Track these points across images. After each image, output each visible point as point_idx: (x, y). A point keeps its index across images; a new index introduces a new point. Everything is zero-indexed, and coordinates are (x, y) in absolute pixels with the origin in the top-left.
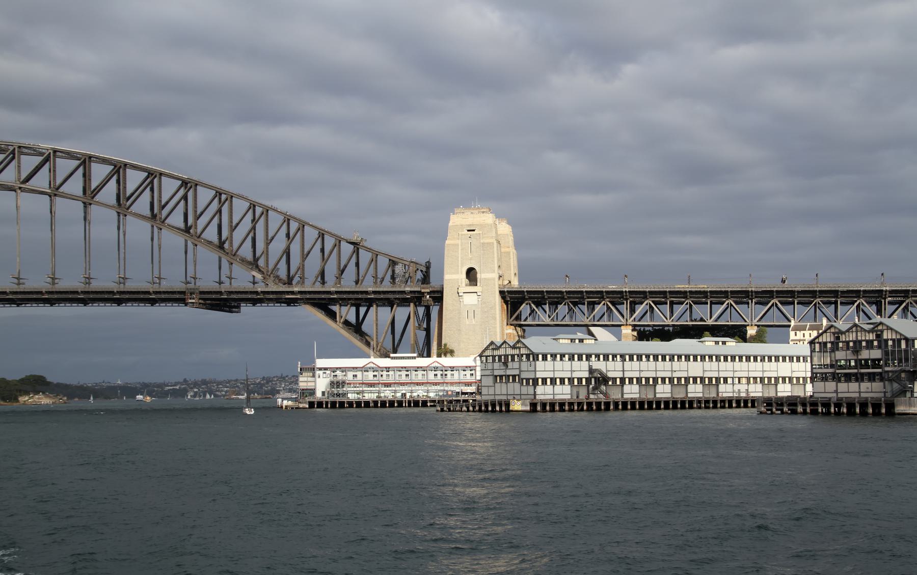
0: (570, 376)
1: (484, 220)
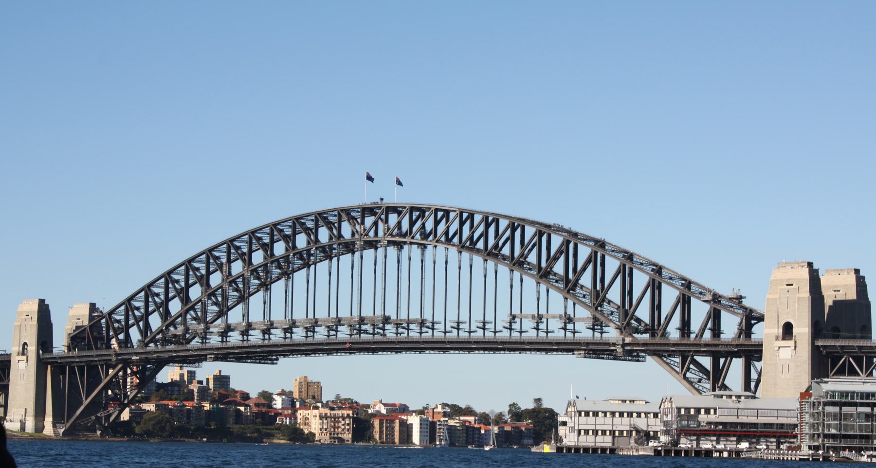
0: (611, 429)
1: (801, 275)
